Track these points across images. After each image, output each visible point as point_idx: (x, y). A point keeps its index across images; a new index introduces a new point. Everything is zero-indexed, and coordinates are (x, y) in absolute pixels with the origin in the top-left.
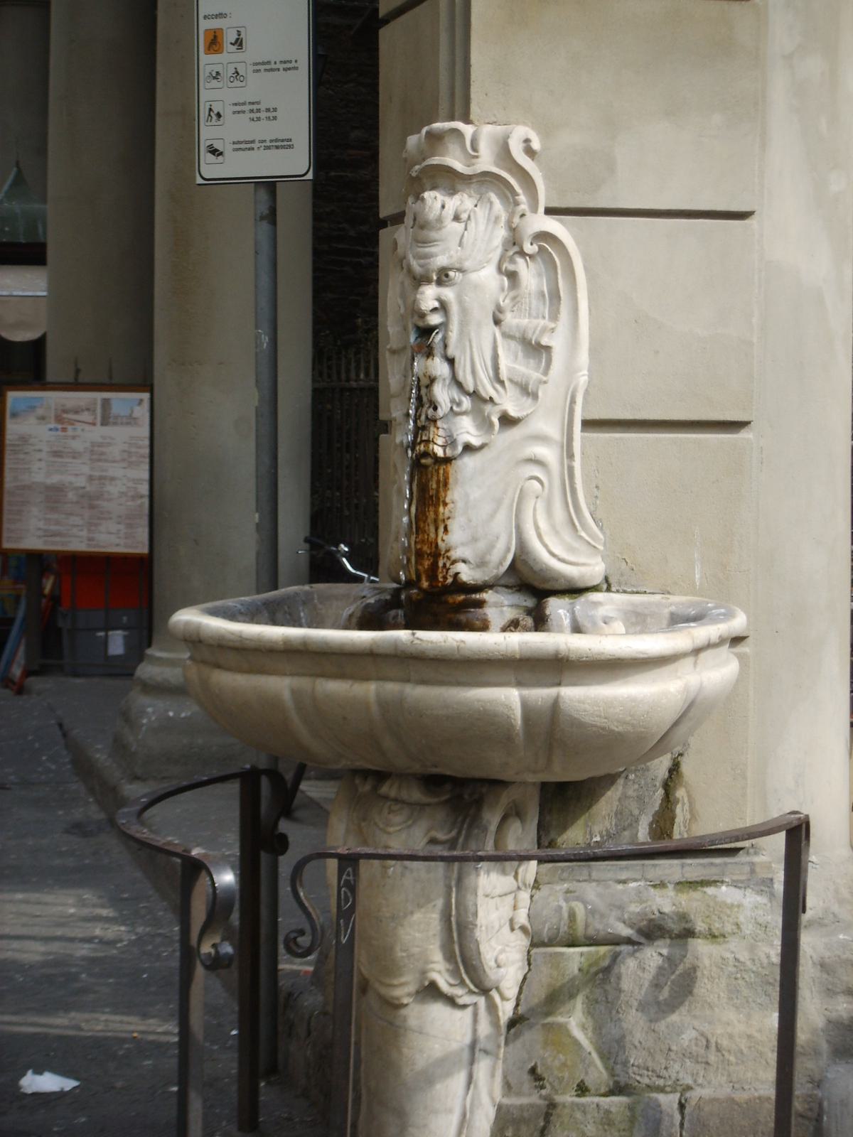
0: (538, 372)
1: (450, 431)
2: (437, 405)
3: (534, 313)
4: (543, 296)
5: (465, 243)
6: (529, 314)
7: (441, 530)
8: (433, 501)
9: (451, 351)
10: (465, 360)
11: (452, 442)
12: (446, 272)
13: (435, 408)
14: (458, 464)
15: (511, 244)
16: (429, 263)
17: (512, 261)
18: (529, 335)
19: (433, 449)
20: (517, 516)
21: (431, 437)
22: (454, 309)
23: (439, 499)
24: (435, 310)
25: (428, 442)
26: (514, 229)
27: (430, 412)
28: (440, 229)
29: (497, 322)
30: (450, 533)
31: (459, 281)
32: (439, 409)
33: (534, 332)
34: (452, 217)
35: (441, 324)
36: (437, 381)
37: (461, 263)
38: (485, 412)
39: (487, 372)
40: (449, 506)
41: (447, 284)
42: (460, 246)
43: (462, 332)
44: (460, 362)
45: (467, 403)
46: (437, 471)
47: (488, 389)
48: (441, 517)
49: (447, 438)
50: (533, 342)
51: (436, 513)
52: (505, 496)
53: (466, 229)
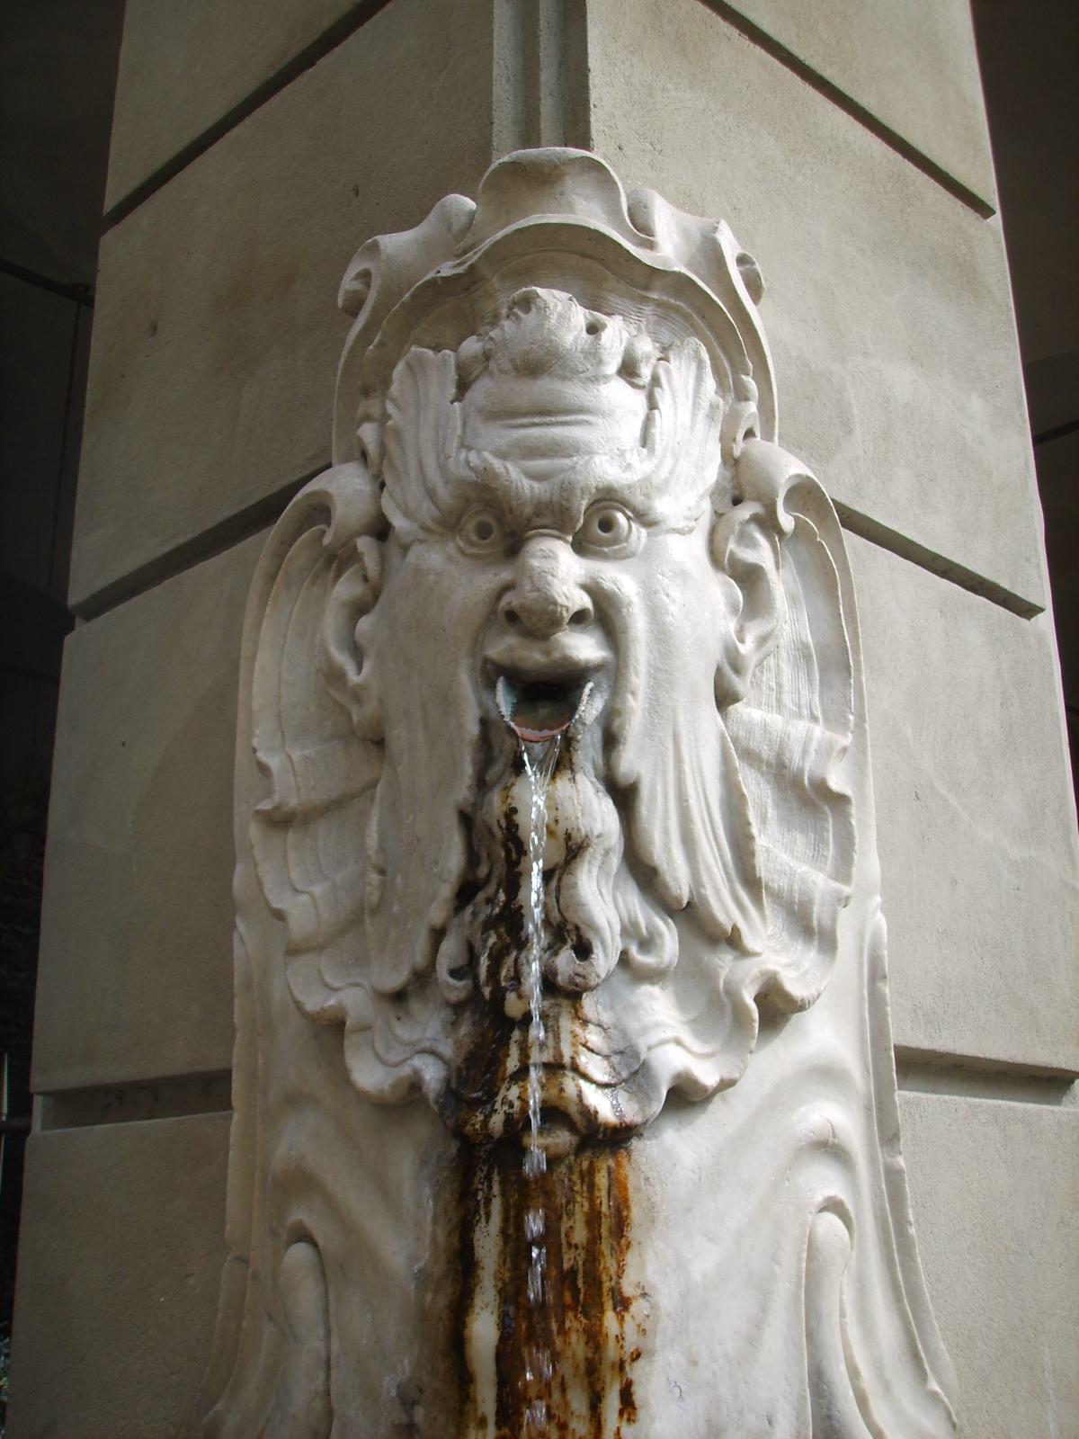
0: (821, 870)
1: (624, 1034)
2: (590, 935)
5: (657, 439)
6: (779, 701)
7: (612, 1402)
8: (575, 1291)
9: (631, 761)
12: (605, 513)
13: (583, 951)
14: (643, 1149)
15: (728, 500)
16: (573, 468)
17: (744, 539)
18: (795, 759)
19: (580, 1095)
20: (810, 1335)
21: (567, 1052)
22: (638, 624)
23: (601, 1283)
24: (579, 618)
25: (555, 1068)
26: (736, 462)
27: (565, 961)
28: (597, 379)
29: (725, 698)
30: (641, 1414)
31: (641, 548)
32: (598, 952)
33: (805, 752)
35: (599, 668)
37: (648, 496)
38: (717, 976)
40: (633, 1308)
42: (643, 447)
46: (589, 1177)
47: (725, 905)
48: (611, 1352)
49: (615, 1059)
51: (594, 1338)
52: (777, 1269)
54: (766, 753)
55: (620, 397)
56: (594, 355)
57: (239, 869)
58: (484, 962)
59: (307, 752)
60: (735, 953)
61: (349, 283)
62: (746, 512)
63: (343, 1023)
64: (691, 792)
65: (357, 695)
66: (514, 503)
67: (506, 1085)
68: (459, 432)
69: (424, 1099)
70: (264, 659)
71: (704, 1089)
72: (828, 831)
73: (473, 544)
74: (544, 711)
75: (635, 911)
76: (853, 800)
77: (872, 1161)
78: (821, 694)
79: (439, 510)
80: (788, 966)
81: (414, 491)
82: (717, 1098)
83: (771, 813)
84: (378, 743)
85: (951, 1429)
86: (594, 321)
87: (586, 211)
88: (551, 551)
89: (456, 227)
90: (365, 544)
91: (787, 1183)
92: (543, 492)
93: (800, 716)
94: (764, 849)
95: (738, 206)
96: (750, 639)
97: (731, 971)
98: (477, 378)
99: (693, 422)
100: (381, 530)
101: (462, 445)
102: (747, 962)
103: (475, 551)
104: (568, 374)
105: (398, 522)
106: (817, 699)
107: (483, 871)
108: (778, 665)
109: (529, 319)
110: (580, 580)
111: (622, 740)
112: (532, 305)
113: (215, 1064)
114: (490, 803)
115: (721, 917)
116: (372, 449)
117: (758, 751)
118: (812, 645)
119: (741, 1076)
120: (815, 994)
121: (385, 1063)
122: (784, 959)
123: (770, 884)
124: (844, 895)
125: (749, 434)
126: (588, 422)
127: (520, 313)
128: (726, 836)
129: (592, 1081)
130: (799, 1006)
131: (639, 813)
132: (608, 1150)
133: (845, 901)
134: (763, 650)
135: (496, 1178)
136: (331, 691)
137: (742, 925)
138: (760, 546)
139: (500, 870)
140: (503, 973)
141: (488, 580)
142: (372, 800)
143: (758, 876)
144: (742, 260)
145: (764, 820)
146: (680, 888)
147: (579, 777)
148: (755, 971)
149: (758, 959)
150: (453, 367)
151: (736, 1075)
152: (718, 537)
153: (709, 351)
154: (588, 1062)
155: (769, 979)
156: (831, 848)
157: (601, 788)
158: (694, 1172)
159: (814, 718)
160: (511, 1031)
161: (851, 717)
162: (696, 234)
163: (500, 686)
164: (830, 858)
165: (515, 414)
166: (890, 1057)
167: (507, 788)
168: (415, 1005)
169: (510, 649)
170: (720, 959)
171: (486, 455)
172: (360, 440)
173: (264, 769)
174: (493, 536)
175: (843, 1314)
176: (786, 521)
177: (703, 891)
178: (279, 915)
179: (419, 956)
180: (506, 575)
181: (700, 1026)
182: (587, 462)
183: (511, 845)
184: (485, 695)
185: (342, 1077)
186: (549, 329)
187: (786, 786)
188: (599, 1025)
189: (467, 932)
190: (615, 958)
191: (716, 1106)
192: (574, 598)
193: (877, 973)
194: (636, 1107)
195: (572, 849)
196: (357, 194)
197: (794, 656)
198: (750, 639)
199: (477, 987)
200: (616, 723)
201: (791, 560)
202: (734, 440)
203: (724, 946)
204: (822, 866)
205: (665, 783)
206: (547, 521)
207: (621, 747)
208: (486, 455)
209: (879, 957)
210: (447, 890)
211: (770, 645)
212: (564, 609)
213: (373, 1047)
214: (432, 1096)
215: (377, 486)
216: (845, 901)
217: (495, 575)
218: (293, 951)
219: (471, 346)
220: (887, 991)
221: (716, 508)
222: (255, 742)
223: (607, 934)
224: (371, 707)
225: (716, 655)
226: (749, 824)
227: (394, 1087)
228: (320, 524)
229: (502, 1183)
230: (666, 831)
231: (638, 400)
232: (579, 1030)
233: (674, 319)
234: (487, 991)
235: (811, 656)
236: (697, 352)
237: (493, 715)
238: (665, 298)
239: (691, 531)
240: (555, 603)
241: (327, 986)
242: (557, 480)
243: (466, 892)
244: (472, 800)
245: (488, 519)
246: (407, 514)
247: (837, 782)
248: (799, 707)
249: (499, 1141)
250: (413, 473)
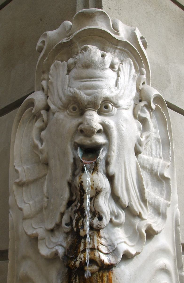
0: (162, 197)
1: (111, 240)
3: (154, 153)
5: (120, 85)
6: (151, 153)
9: (113, 169)
10: (122, 178)
11: (114, 251)
14: (116, 270)
15: (138, 101)
16: (98, 92)
17: (142, 111)
18: (155, 168)
19: (99, 256)
21: (96, 245)
22: (115, 133)
24: (99, 132)
25: (93, 249)
26: (140, 91)
27: (96, 221)
28: (104, 69)
29: (137, 153)
31: (115, 113)
32: (104, 219)
33: (158, 167)
35: (104, 144)
36: (101, 194)
37: (117, 100)
38: (135, 225)
42: (116, 87)
43: (119, 155)
44: (118, 179)
45: (123, 215)
46: (102, 278)
47: (137, 207)
49: (109, 247)
54: (148, 167)
55: (110, 74)
56: (103, 63)
57: (10, 197)
58: (74, 221)
59: (28, 167)
60: (140, 219)
61: (39, 44)
62: (143, 104)
63: (37, 238)
64: (128, 177)
65: (41, 152)
66: (82, 101)
67: (80, 254)
68: (68, 83)
69: (59, 257)
70: (17, 142)
71: (132, 255)
72: (164, 187)
73: (71, 112)
74: (90, 156)
75: (114, 208)
76: (171, 179)
77: (176, 274)
78: (162, 151)
79: (63, 103)
80: (154, 222)
81: (56, 98)
82: (135, 257)
83: (149, 183)
84: (47, 164)
86: (103, 54)
87: (101, 25)
88: (92, 114)
89: (67, 29)
90: (43, 112)
91: (153, 279)
92: (90, 99)
93: (157, 157)
94: (147, 192)
95: (141, 24)
96: (144, 137)
97: (139, 224)
98: (72, 69)
99: (129, 81)
100: (47, 108)
101: (69, 86)
102: (143, 222)
103: (72, 114)
104: (96, 68)
105: (52, 106)
106: (161, 153)
107: (74, 198)
108: (151, 144)
109: (86, 53)
110: (99, 122)
111: (110, 164)
112: (87, 50)
113: (4, 248)
114: (76, 180)
115: (136, 210)
116: (45, 87)
117: (146, 166)
118: (160, 138)
119: (141, 252)
120: (161, 230)
121: (48, 248)
122: (153, 221)
123: (149, 201)
124: (168, 204)
125: (144, 83)
126: (101, 80)
127: (84, 52)
128: (138, 188)
129: (102, 253)
130: (157, 233)
131: (115, 182)
132: (107, 271)
133: (169, 206)
134: (147, 140)
135: (77, 278)
136: (34, 151)
137: (142, 212)
138: (146, 113)
139: (79, 197)
140: (79, 224)
141: (75, 122)
142: (45, 179)
143: (146, 199)
144: (142, 38)
145: (147, 184)
146: (126, 202)
147: (99, 173)
148: (145, 224)
150: (66, 66)
151: (140, 251)
152: (136, 111)
153: (133, 62)
154: (102, 248)
155: (149, 226)
156: (165, 192)
157: (105, 176)
158: (129, 276)
159: (161, 158)
160: (81, 239)
161: (170, 158)
162: (130, 31)
163: (79, 149)
164: (165, 194)
165: (82, 78)
166: (180, 246)
167: (80, 176)
168: (56, 233)
169: (81, 140)
170: (136, 221)
171: (75, 89)
172: (42, 85)
173: (17, 171)
174: (77, 110)
176: (153, 106)
177: (132, 203)
178: (21, 209)
179: (57, 220)
180: (80, 120)
181: (131, 238)
182: (101, 91)
183: (81, 191)
184: (75, 152)
185: (37, 252)
186: (91, 56)
188: (104, 238)
189: (70, 214)
190: (109, 220)
191: (135, 259)
193: (177, 225)
194: (114, 259)
195: (97, 192)
196: (41, 21)
197: (155, 142)
198: (144, 137)
199: (72, 228)
200: (109, 159)
201: (155, 117)
202: (140, 85)
203: (137, 217)
204: (163, 196)
205: (122, 175)
206: (91, 106)
207: (110, 165)
208: (75, 89)
209: (177, 220)
210: (65, 203)
211: (149, 139)
212: (95, 129)
213: (45, 244)
214: (61, 257)
215: (46, 97)
216: (169, 206)
217: (77, 120)
218: (24, 219)
219: (71, 60)
220: (180, 229)
222: (15, 164)
223: (107, 214)
224: (45, 155)
225: (135, 141)
226: (143, 185)
227: (51, 254)
228: (31, 107)
229: (79, 279)
230: (122, 187)
231: (115, 75)
232: (99, 239)
234: (75, 229)
235: (160, 141)
236: (130, 62)
237: (77, 157)
238: (122, 48)
239: (128, 109)
240: (93, 128)
241: (33, 228)
242: (93, 95)
243: (70, 203)
244: (71, 179)
245: (75, 105)
246: (54, 104)
247: (167, 175)
248: (157, 155)
249: (78, 268)
250: (56, 94)
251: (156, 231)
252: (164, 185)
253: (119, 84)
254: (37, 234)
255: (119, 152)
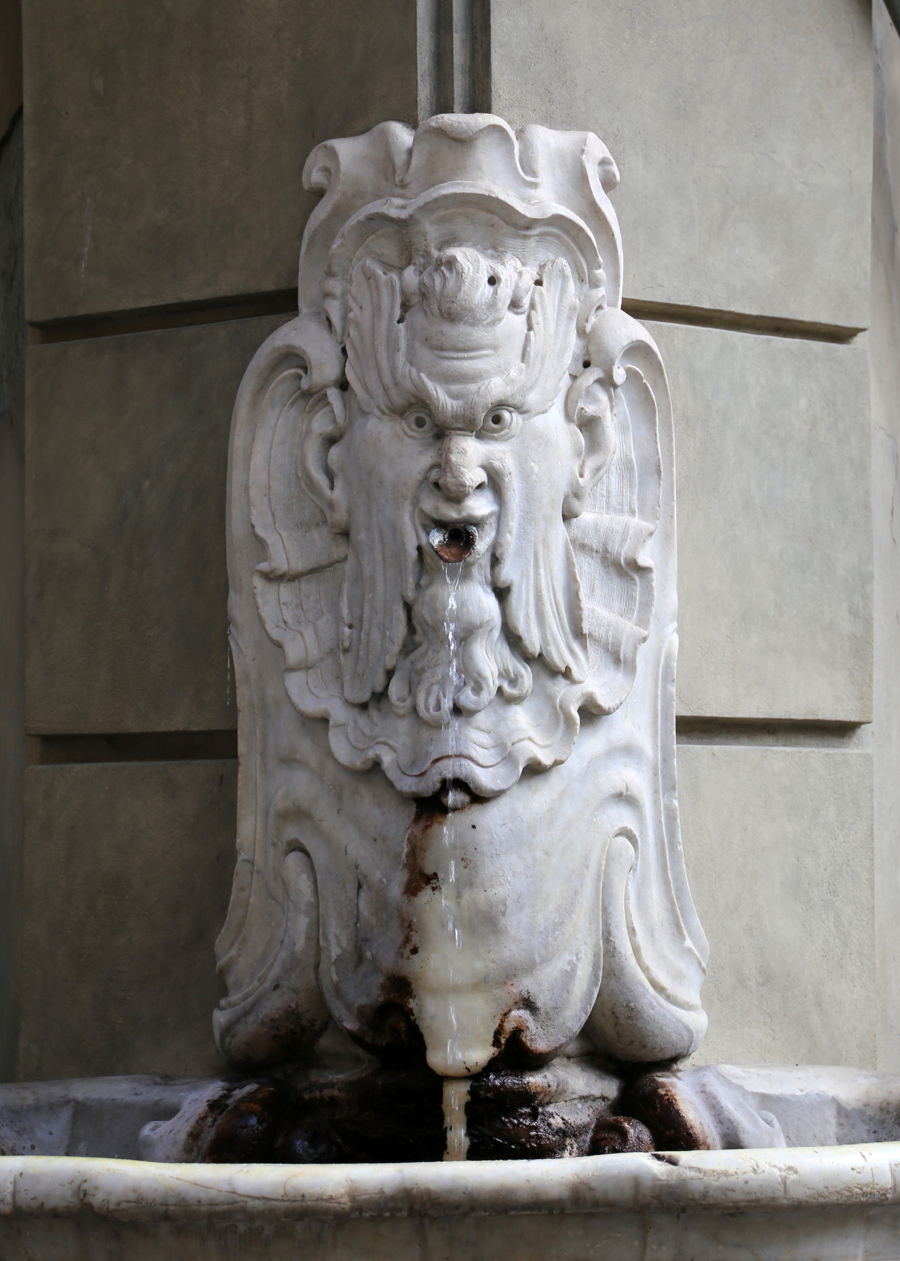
0: (630, 619)
3: (614, 501)
4: (630, 469)
5: (532, 354)
6: (608, 503)
9: (508, 572)
12: (497, 413)
13: (478, 688)
16: (478, 392)
20: (605, 910)
24: (480, 487)
28: (493, 323)
29: (568, 516)
33: (624, 540)
34: (508, 302)
38: (556, 697)
39: (559, 615)
41: (496, 435)
45: (526, 674)
50: (622, 562)
53: (530, 328)
56: (492, 305)
60: (568, 682)
72: (636, 592)
75: (507, 663)
76: (654, 570)
77: (656, 802)
84: (345, 534)
85: (701, 973)
86: (494, 275)
88: (463, 449)
90: (333, 395)
93: (622, 511)
99: (557, 325)
100: (343, 385)
106: (635, 497)
108: (609, 478)
110: (480, 463)
111: (503, 562)
118: (634, 460)
120: (618, 702)
123: (593, 634)
124: (643, 636)
127: (445, 271)
131: (511, 604)
138: (600, 401)
143: (584, 633)
144: (603, 162)
148: (579, 694)
149: (582, 684)
152: (572, 396)
159: (632, 512)
166: (673, 736)
170: (558, 687)
174: (425, 426)
175: (627, 898)
176: (619, 375)
177: (549, 648)
185: (330, 753)
187: (608, 565)
190: (494, 691)
192: (474, 476)
204: (630, 616)
206: (460, 426)
207: (502, 566)
212: (470, 488)
218: (292, 670)
221: (571, 372)
225: (563, 487)
230: (527, 615)
233: (548, 240)
235: (633, 467)
247: (644, 560)
251: (604, 708)
252: (635, 587)
253: (529, 353)
254: (326, 711)
255: (523, 529)
